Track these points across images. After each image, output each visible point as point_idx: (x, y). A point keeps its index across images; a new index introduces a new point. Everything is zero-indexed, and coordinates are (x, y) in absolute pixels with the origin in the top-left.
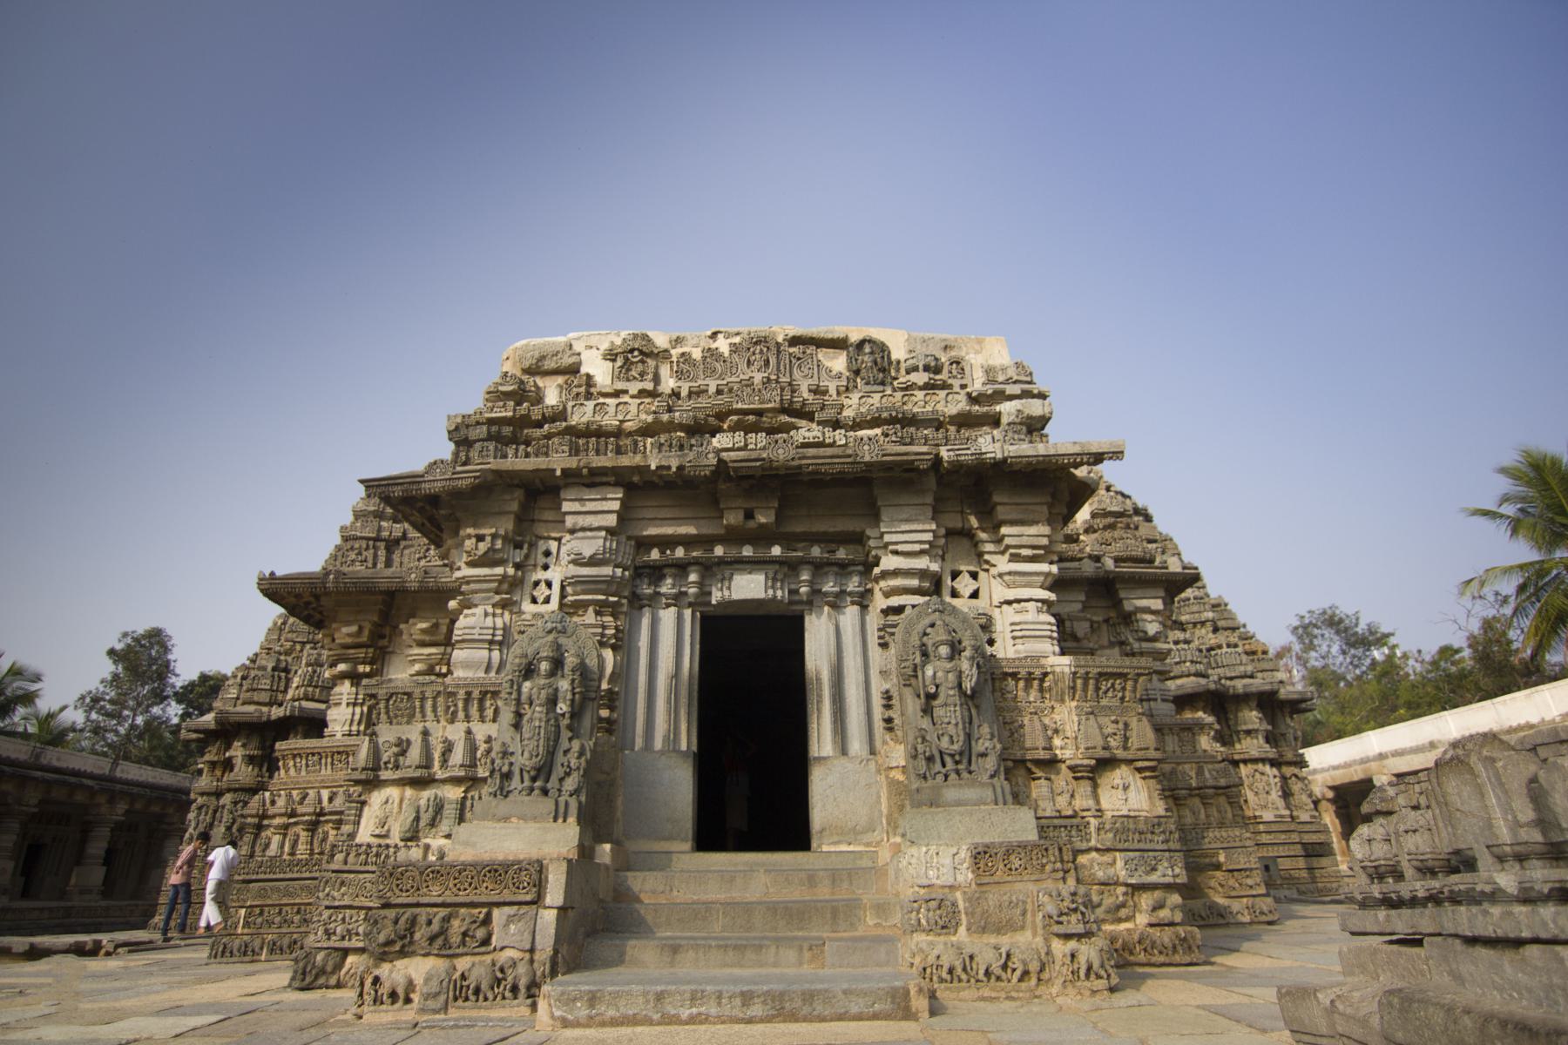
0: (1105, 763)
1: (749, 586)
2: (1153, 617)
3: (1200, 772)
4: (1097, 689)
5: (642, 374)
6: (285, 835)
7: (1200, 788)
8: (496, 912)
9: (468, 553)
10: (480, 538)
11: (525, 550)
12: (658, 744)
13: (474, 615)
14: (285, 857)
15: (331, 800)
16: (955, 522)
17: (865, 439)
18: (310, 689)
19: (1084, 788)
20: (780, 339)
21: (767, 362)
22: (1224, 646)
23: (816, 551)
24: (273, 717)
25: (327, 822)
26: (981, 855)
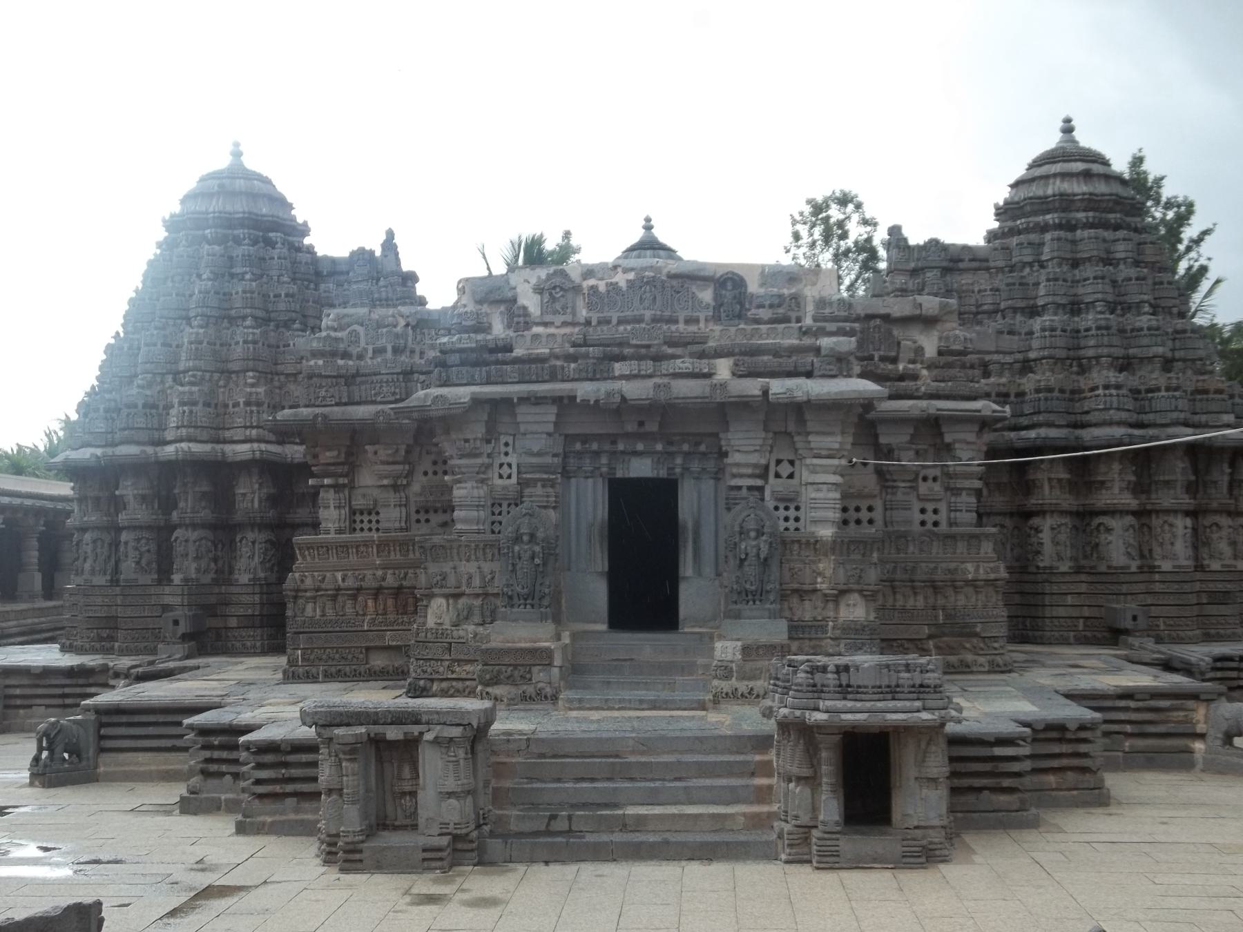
0: (843, 593)
1: (641, 468)
4: (848, 548)
5: (564, 308)
6: (315, 603)
8: (535, 669)
9: (459, 449)
13: (463, 488)
14: (318, 617)
15: (343, 580)
17: (718, 386)
19: (831, 605)
20: (664, 278)
22: (1163, 388)
23: (686, 447)
24: (161, 459)
25: (343, 595)
26: (746, 650)
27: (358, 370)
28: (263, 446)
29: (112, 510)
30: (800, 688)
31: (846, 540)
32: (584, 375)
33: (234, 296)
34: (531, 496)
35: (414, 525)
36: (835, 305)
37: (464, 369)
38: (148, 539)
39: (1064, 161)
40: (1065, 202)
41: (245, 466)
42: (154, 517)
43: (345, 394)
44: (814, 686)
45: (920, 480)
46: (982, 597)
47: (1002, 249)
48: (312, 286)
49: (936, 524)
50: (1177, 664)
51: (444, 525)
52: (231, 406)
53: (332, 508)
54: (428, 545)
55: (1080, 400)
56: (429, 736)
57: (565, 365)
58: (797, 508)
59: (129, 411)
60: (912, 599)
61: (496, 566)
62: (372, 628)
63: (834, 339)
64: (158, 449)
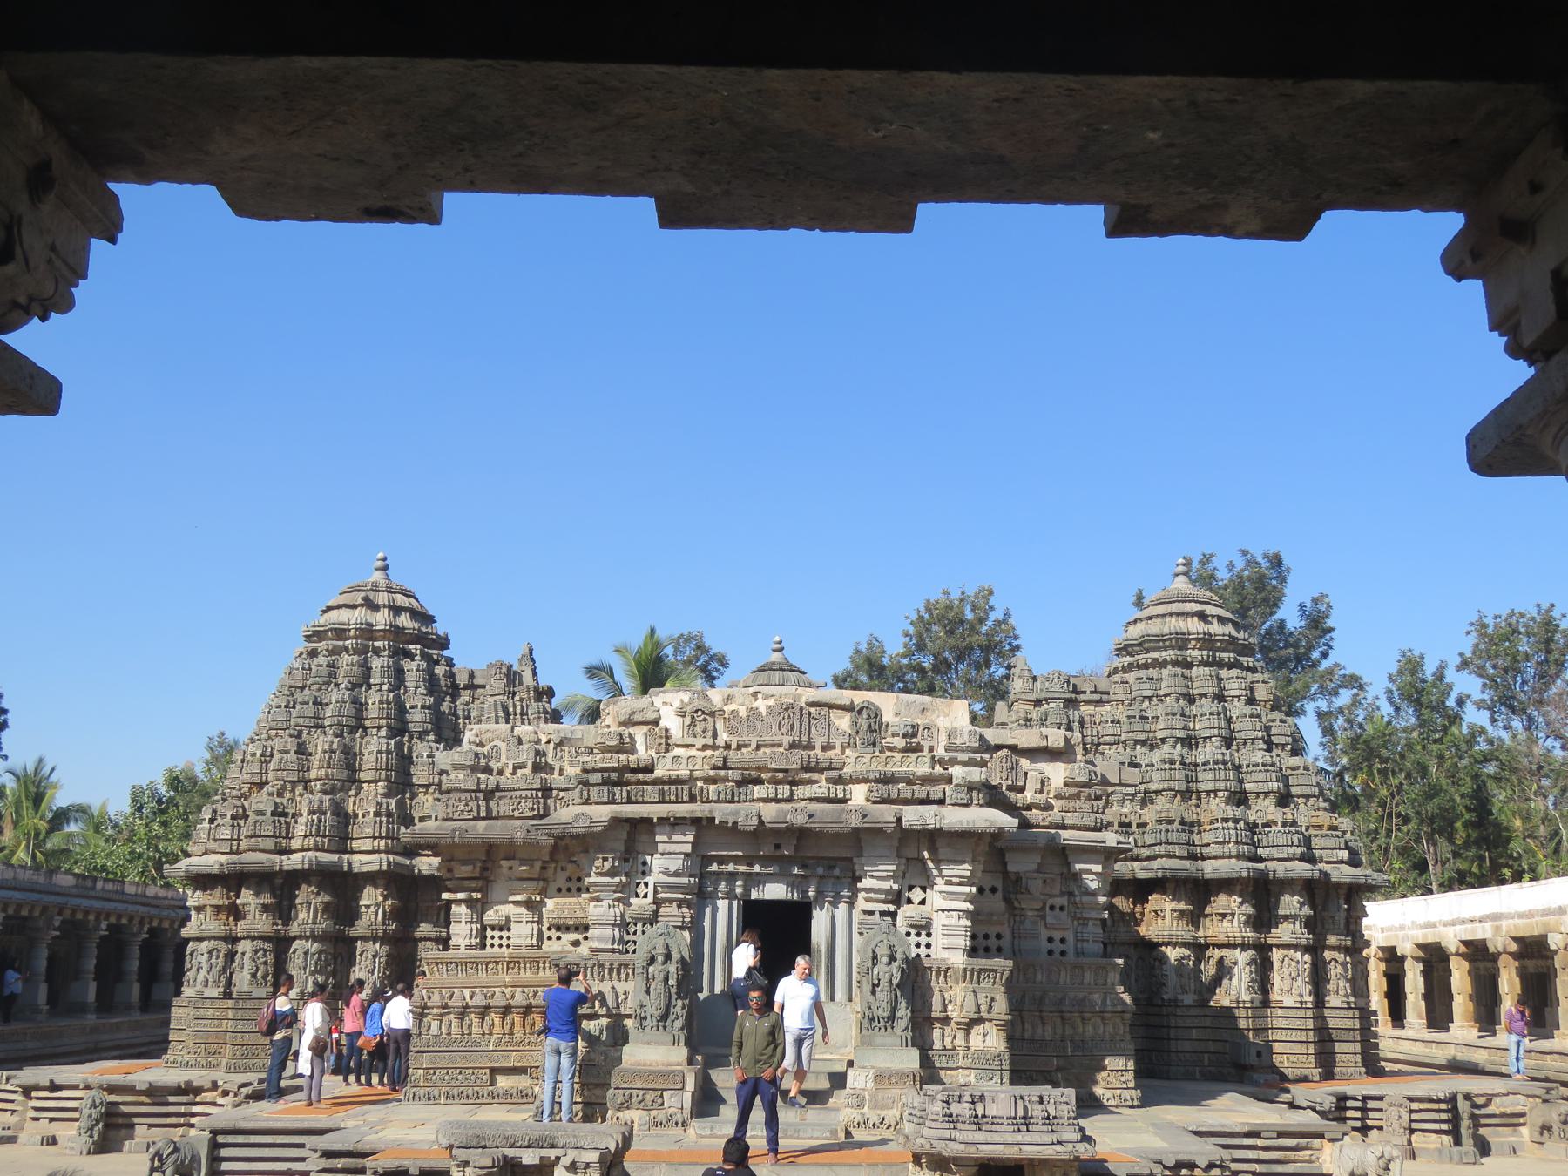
1: (775, 891)
2: (1094, 877)
3: (1104, 1000)
4: (979, 978)
6: (441, 1021)
7: (1103, 1012)
8: (665, 1093)
9: (597, 868)
10: (605, 859)
11: (631, 863)
12: (718, 990)
15: (471, 998)
16: (911, 853)
18: (319, 839)
20: (803, 705)
21: (792, 728)
24: (286, 868)
25: (471, 1013)
26: (879, 1077)
27: (498, 785)
28: (391, 858)
29: (231, 919)
30: (935, 1117)
31: (977, 968)
32: (722, 797)
33: (370, 706)
34: (665, 916)
35: (547, 946)
36: (966, 738)
37: (605, 788)
38: (265, 951)
39: (1179, 602)
40: (1181, 640)
41: (371, 878)
42: (275, 927)
43: (483, 809)
44: (951, 1115)
45: (1047, 909)
46: (1110, 1029)
47: (1122, 682)
48: (448, 698)
49: (1063, 953)
50: (1304, 1104)
51: (576, 943)
52: (360, 816)
53: (463, 923)
54: (562, 964)
55: (1199, 832)
56: (566, 1161)
57: (705, 786)
58: (929, 935)
59: (258, 818)
60: (1039, 1031)
61: (630, 986)
62: (498, 1048)
63: (966, 769)
64: (283, 857)
